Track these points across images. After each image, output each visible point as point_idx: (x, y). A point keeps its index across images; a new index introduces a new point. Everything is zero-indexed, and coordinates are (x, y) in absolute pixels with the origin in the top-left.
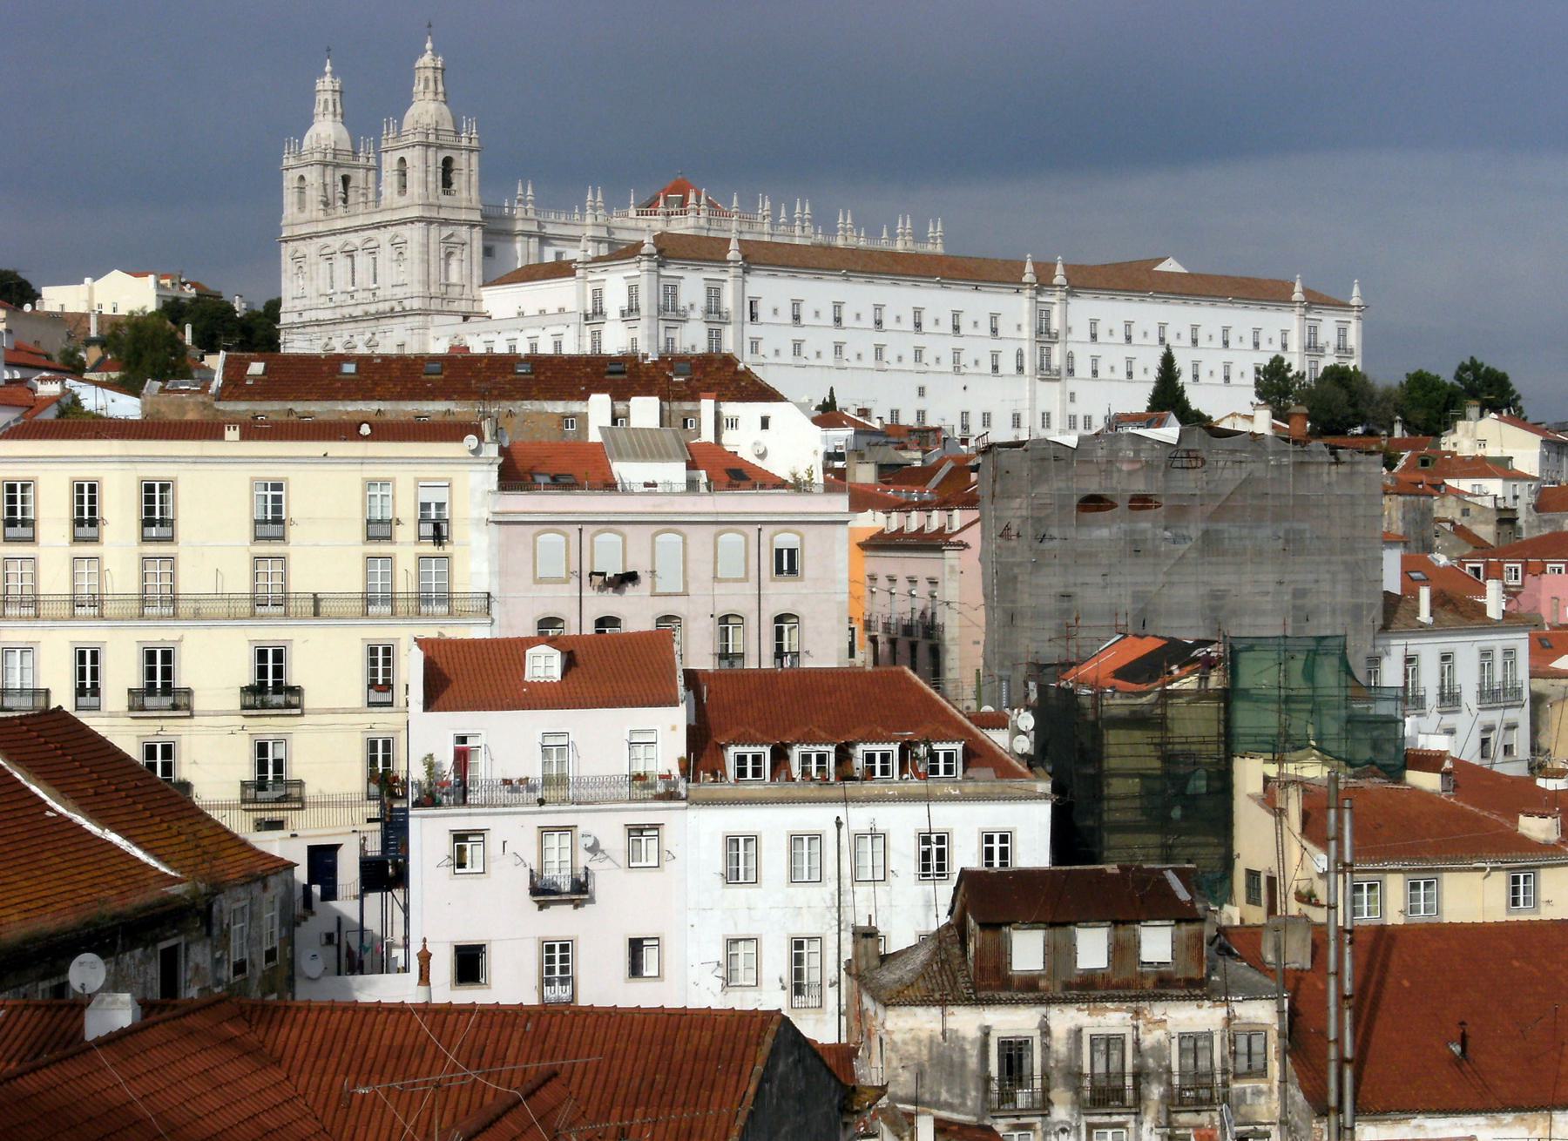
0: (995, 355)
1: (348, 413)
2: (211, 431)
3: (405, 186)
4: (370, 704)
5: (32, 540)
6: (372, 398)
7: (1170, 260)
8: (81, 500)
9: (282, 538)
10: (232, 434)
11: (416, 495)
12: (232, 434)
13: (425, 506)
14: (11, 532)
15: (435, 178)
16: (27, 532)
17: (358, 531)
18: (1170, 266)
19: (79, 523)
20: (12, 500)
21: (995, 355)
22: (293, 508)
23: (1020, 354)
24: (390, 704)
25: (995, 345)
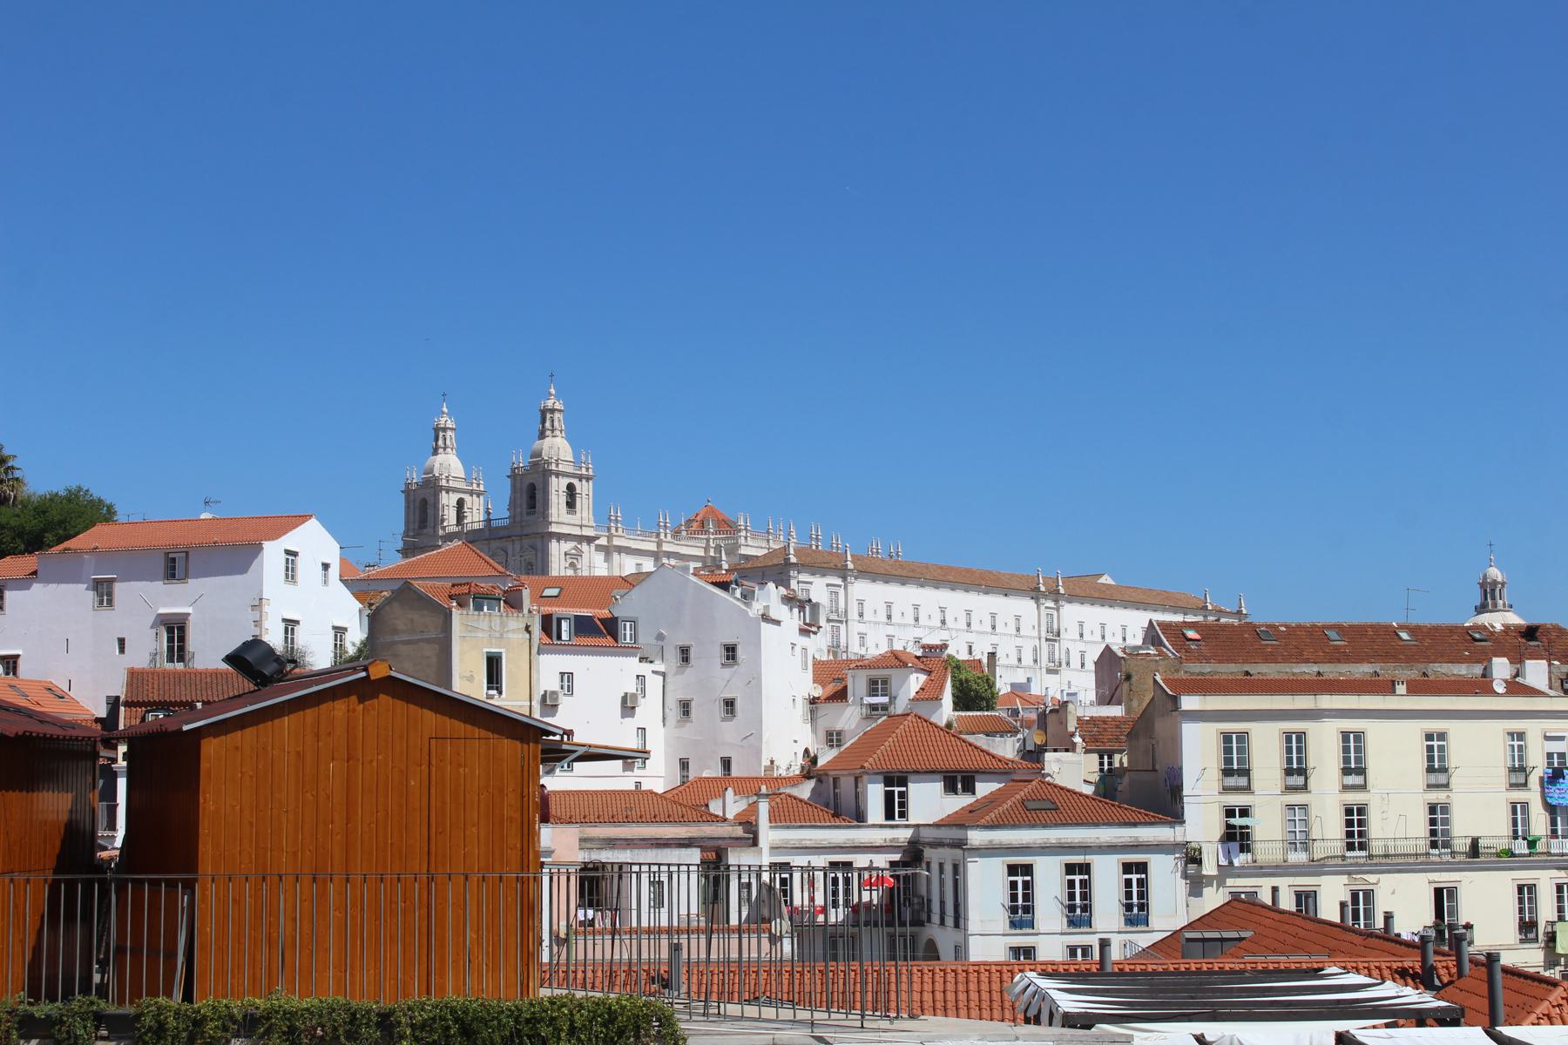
0: (1019, 649)
1: (1294, 674)
2: (1388, 688)
3: (535, 508)
4: (1522, 941)
5: (1248, 789)
6: (1307, 661)
7: (1105, 577)
8: (1289, 750)
9: (1447, 786)
10: (1401, 689)
11: (1543, 748)
12: (1401, 689)
13: (1550, 756)
14: (1232, 781)
15: (563, 499)
16: (1242, 781)
17: (1501, 777)
18: (1106, 580)
19: (1289, 772)
20: (1228, 750)
21: (1019, 649)
22: (1453, 760)
23: (1035, 650)
24: (1536, 940)
25: (1019, 642)
